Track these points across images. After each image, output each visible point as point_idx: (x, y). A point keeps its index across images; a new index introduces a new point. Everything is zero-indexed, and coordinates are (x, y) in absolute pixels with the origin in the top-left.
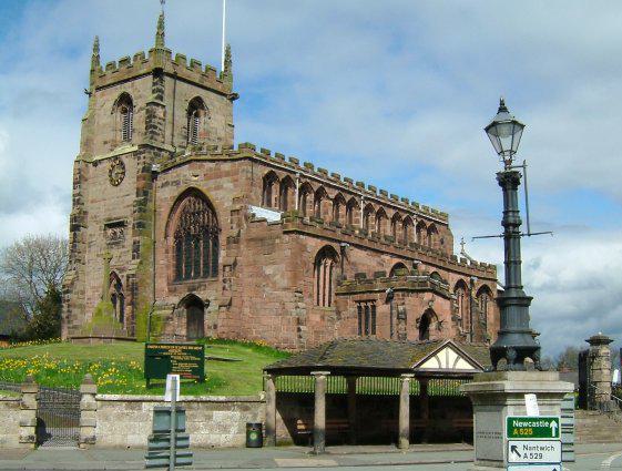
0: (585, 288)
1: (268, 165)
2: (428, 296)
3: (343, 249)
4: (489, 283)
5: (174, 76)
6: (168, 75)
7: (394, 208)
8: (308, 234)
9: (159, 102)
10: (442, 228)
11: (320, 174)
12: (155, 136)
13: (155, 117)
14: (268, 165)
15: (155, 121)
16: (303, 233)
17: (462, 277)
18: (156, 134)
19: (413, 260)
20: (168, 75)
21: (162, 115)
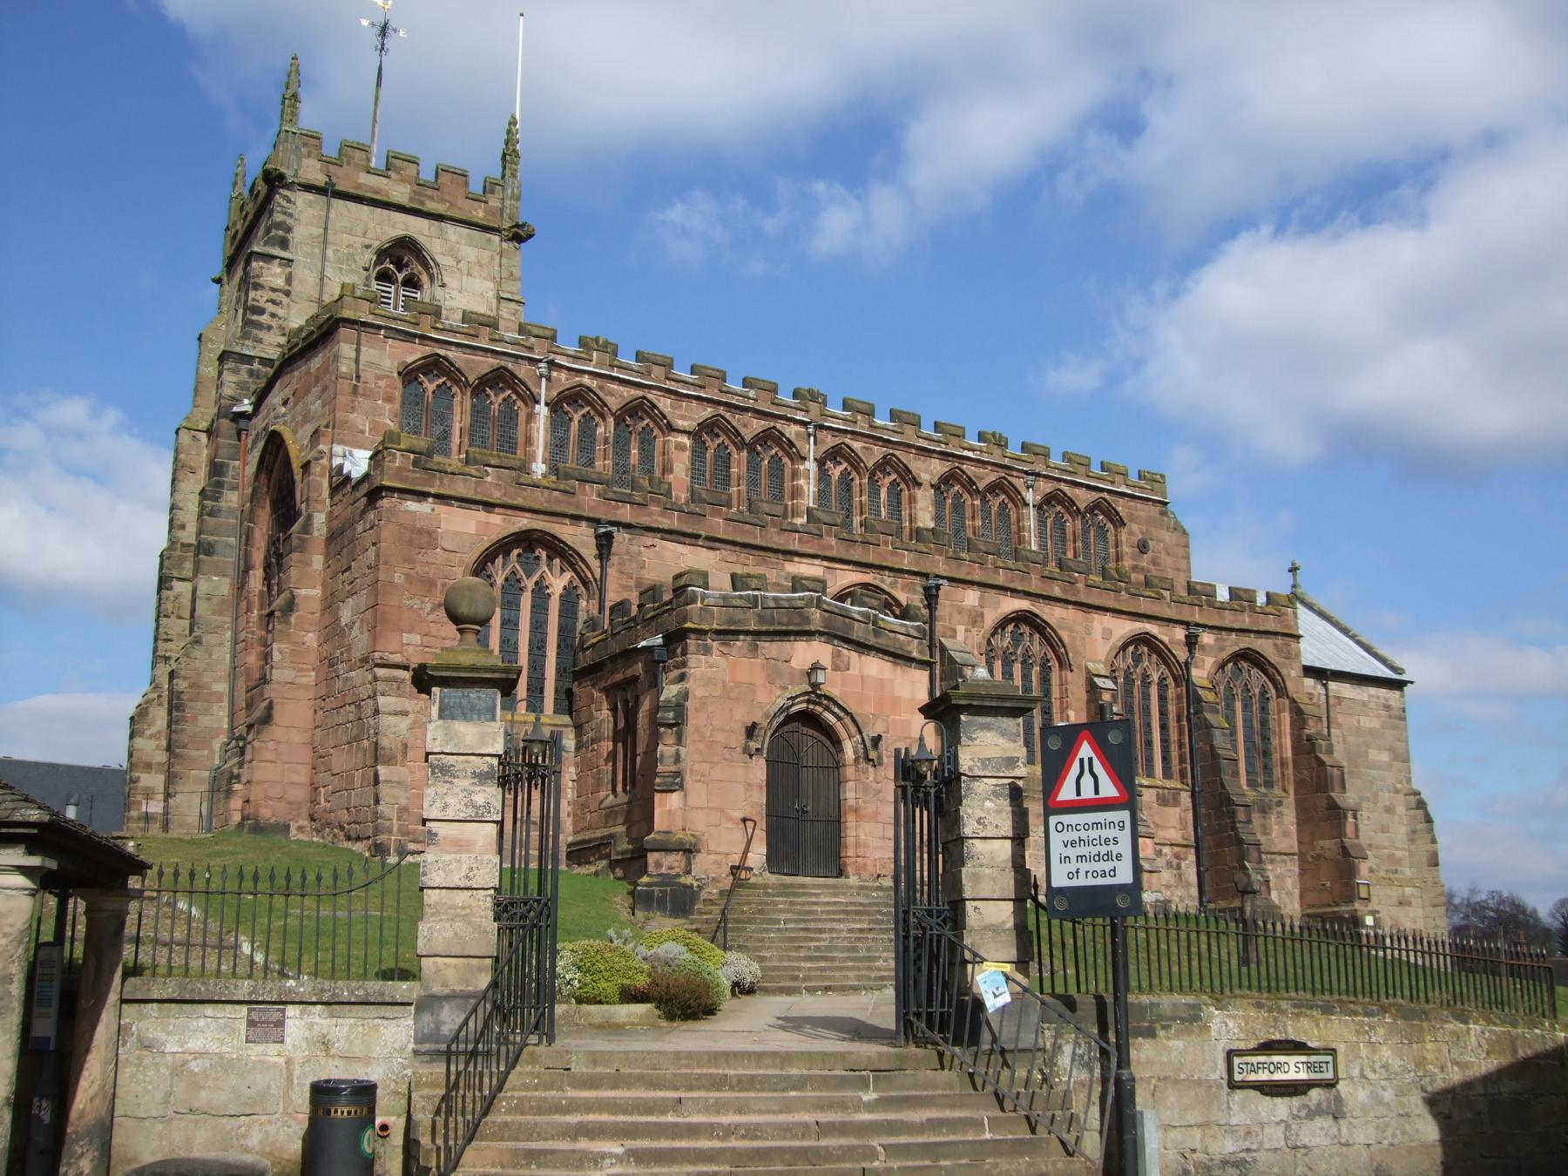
0: (1117, 540)
1: (424, 338)
2: (805, 653)
3: (604, 544)
4: (1265, 646)
5: (328, 191)
6: (308, 188)
7: (944, 456)
8: (442, 498)
9: (276, 251)
10: (1144, 510)
11: (1024, 456)
12: (262, 334)
13: (257, 286)
14: (424, 338)
15: (258, 297)
16: (421, 496)
17: (1153, 628)
18: (259, 326)
19: (926, 576)
20: (308, 188)
21: (280, 282)
